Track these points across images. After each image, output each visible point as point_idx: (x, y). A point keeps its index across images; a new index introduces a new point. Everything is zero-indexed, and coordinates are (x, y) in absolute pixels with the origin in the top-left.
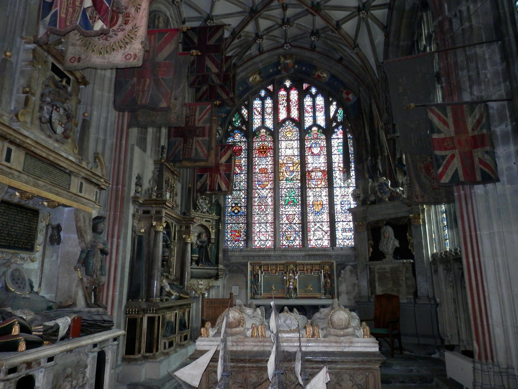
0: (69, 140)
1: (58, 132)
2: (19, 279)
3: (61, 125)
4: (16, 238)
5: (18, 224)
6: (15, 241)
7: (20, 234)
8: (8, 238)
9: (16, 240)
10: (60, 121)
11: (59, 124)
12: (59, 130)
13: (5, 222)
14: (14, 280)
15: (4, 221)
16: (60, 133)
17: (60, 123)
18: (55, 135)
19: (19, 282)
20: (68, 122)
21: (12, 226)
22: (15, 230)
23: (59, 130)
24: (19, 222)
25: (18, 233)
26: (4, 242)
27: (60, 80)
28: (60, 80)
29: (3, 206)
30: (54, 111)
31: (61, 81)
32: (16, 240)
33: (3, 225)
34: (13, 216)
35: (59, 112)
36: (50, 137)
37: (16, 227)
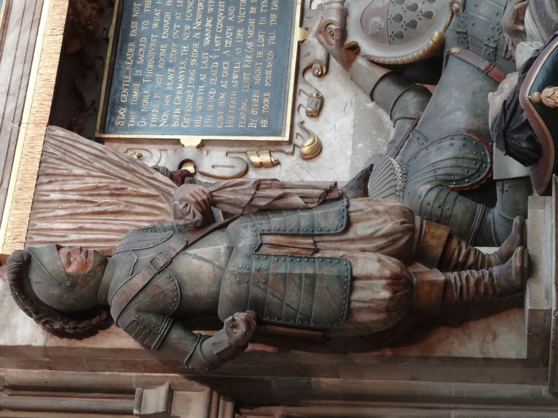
2: (399, 18)
4: (245, 25)
5: (191, 23)
6: (258, 27)
7: (232, 9)
8: (248, 58)
9: (252, 22)
13: (187, 75)
14: (400, 36)
15: (186, 82)
19: (409, 17)
21: (202, 49)
22: (213, 32)
24: (183, 22)
25: (226, 22)
26: (264, 68)
29: (130, 93)
32: (252, 22)
33: (198, 83)
34: (163, 48)
37: (203, 30)
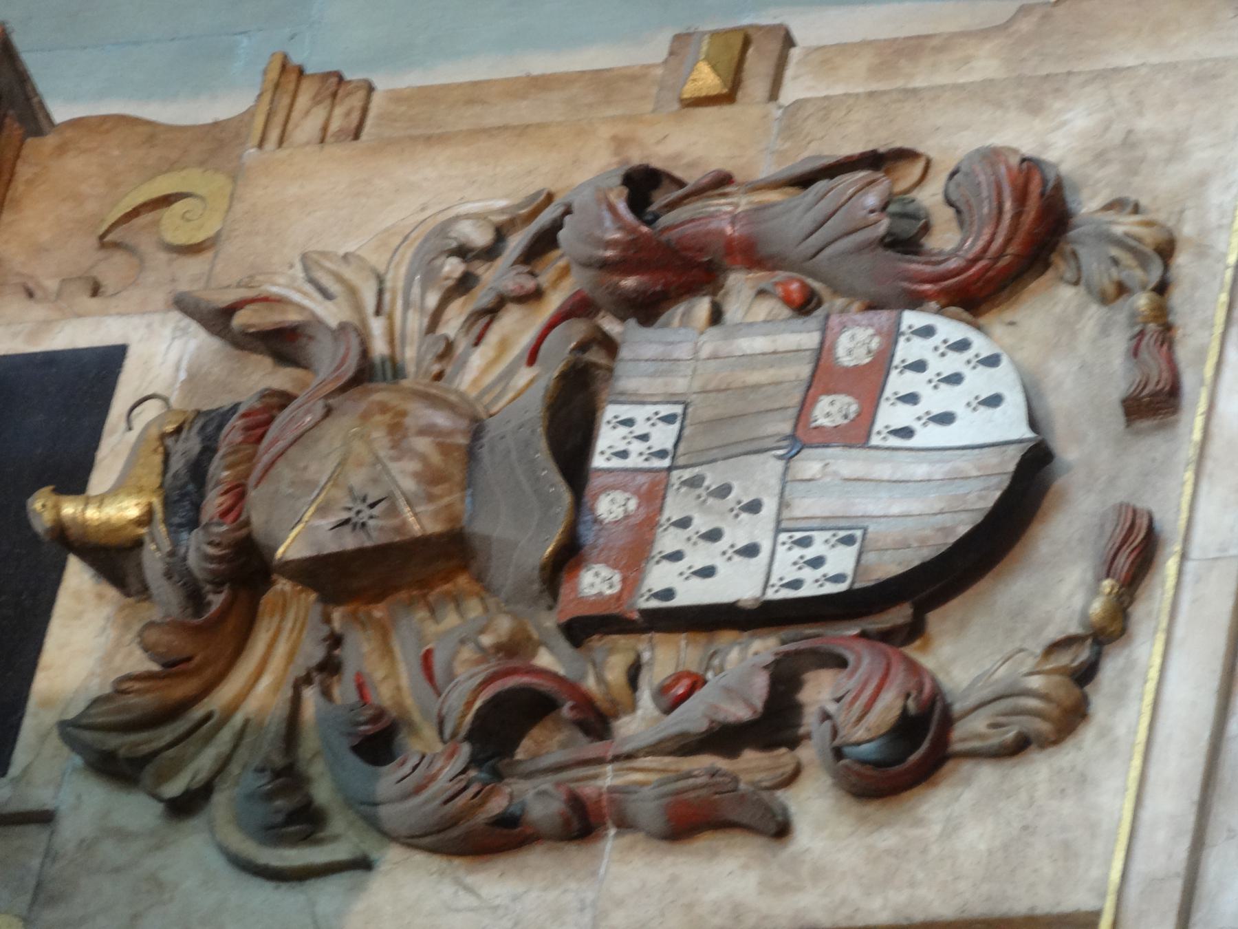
0: (1061, 136)
1: (1010, 424)
3: (869, 382)
10: (802, 437)
11: (856, 434)
12: (954, 403)
16: (1004, 379)
17: (831, 410)
18: (1068, 452)
20: (751, 254)
23: (954, 403)
27: (77, 577)
28: (77, 577)
30: (674, 581)
31: (114, 558)
35: (653, 493)
36: (1136, 554)
